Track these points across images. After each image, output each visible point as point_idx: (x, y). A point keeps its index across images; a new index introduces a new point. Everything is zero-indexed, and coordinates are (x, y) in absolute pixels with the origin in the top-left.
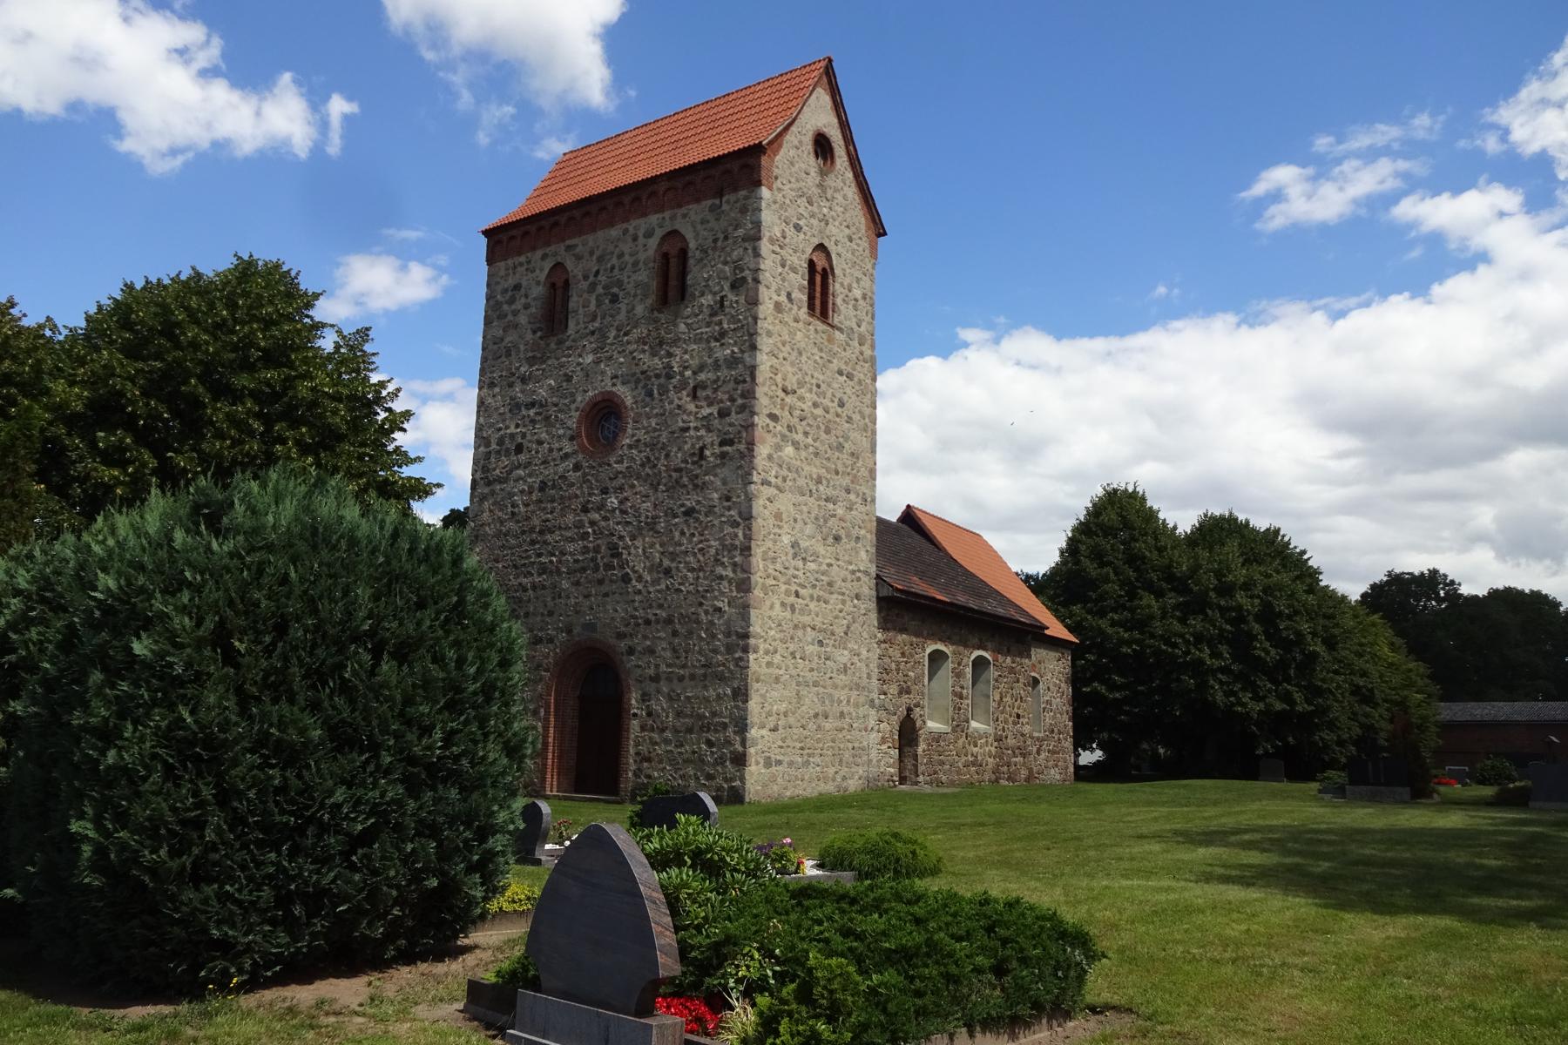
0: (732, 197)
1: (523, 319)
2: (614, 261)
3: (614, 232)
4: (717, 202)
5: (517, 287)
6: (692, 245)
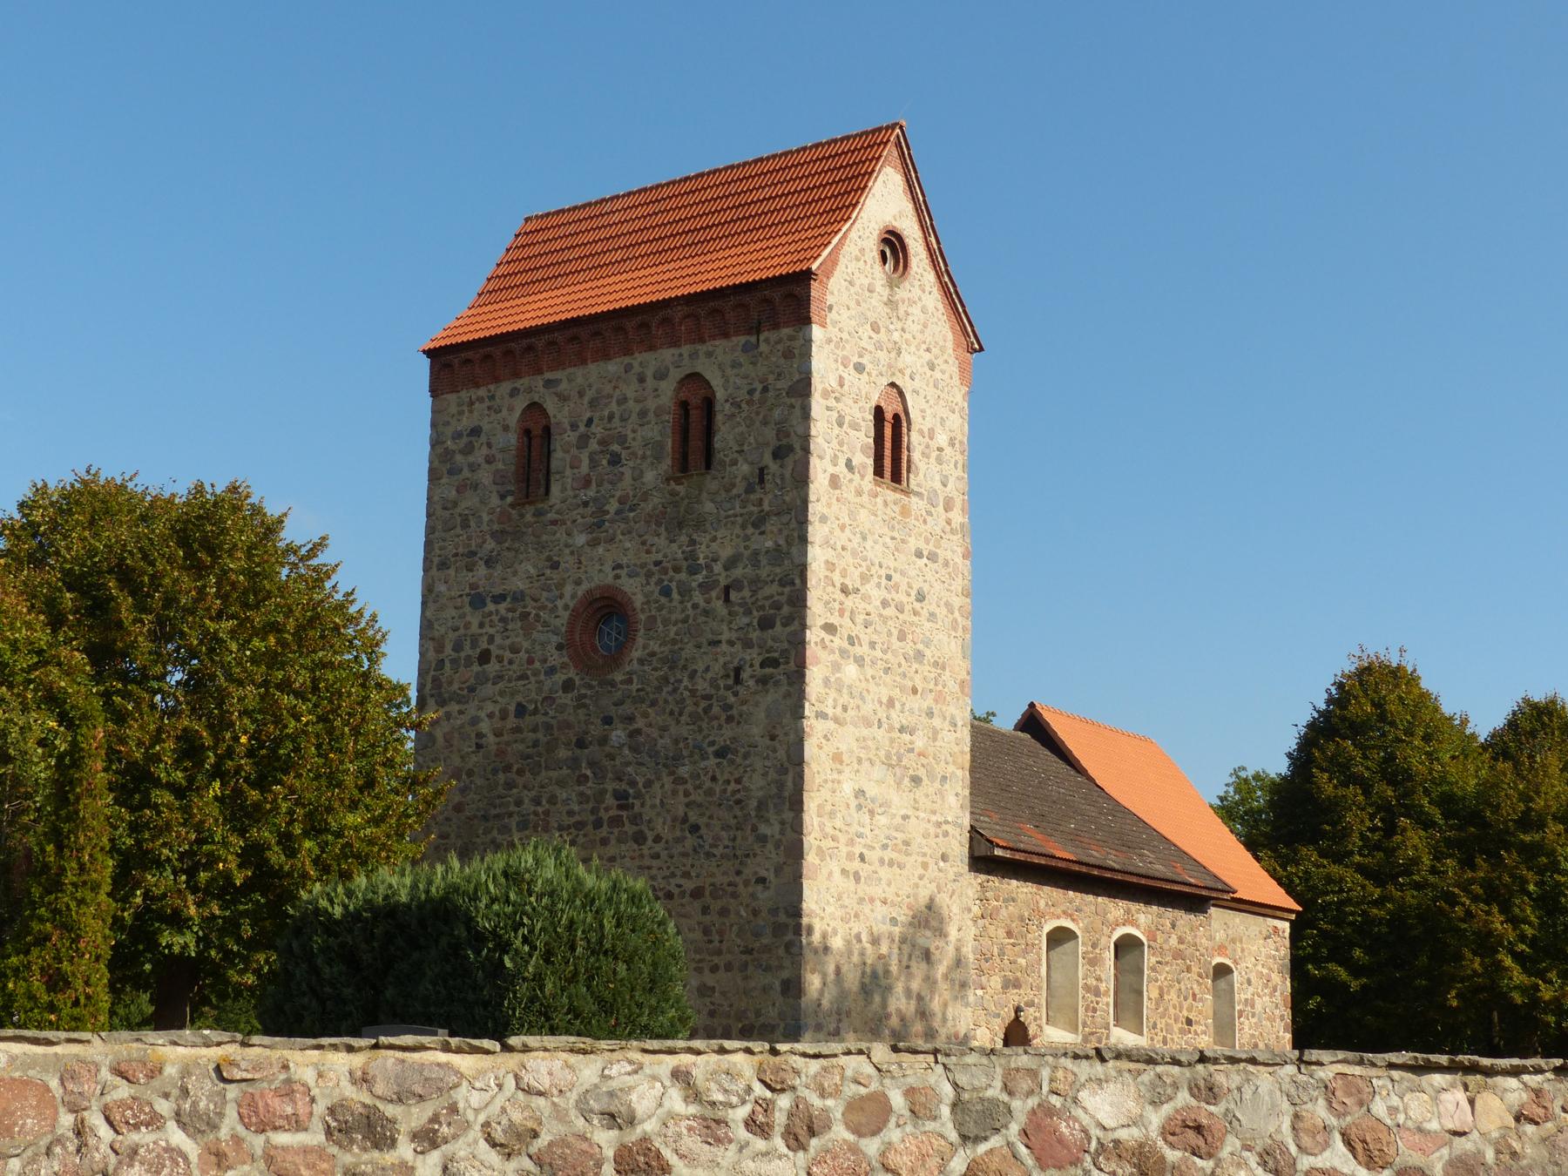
0: (773, 336)
1: (485, 476)
2: (614, 407)
3: (613, 367)
4: (753, 339)
5: (476, 432)
6: (720, 394)
